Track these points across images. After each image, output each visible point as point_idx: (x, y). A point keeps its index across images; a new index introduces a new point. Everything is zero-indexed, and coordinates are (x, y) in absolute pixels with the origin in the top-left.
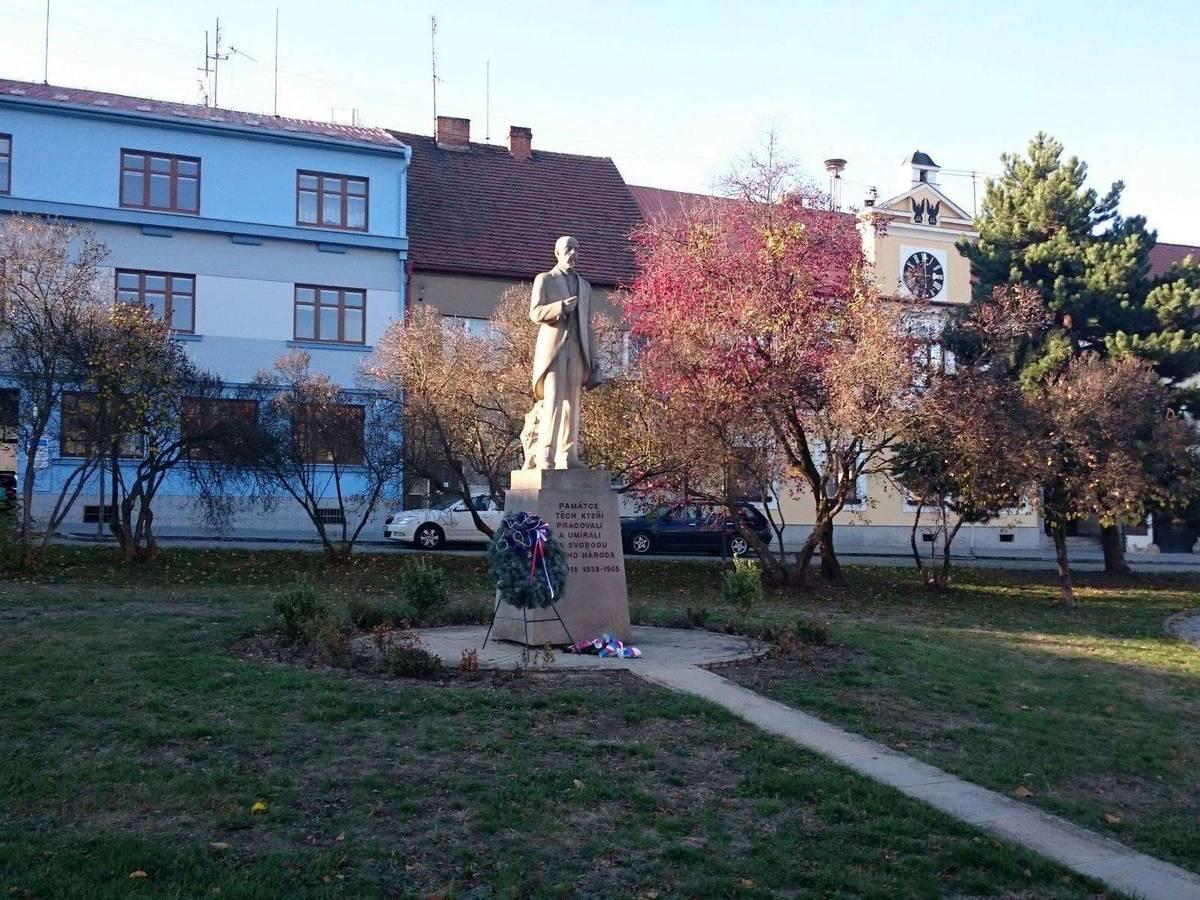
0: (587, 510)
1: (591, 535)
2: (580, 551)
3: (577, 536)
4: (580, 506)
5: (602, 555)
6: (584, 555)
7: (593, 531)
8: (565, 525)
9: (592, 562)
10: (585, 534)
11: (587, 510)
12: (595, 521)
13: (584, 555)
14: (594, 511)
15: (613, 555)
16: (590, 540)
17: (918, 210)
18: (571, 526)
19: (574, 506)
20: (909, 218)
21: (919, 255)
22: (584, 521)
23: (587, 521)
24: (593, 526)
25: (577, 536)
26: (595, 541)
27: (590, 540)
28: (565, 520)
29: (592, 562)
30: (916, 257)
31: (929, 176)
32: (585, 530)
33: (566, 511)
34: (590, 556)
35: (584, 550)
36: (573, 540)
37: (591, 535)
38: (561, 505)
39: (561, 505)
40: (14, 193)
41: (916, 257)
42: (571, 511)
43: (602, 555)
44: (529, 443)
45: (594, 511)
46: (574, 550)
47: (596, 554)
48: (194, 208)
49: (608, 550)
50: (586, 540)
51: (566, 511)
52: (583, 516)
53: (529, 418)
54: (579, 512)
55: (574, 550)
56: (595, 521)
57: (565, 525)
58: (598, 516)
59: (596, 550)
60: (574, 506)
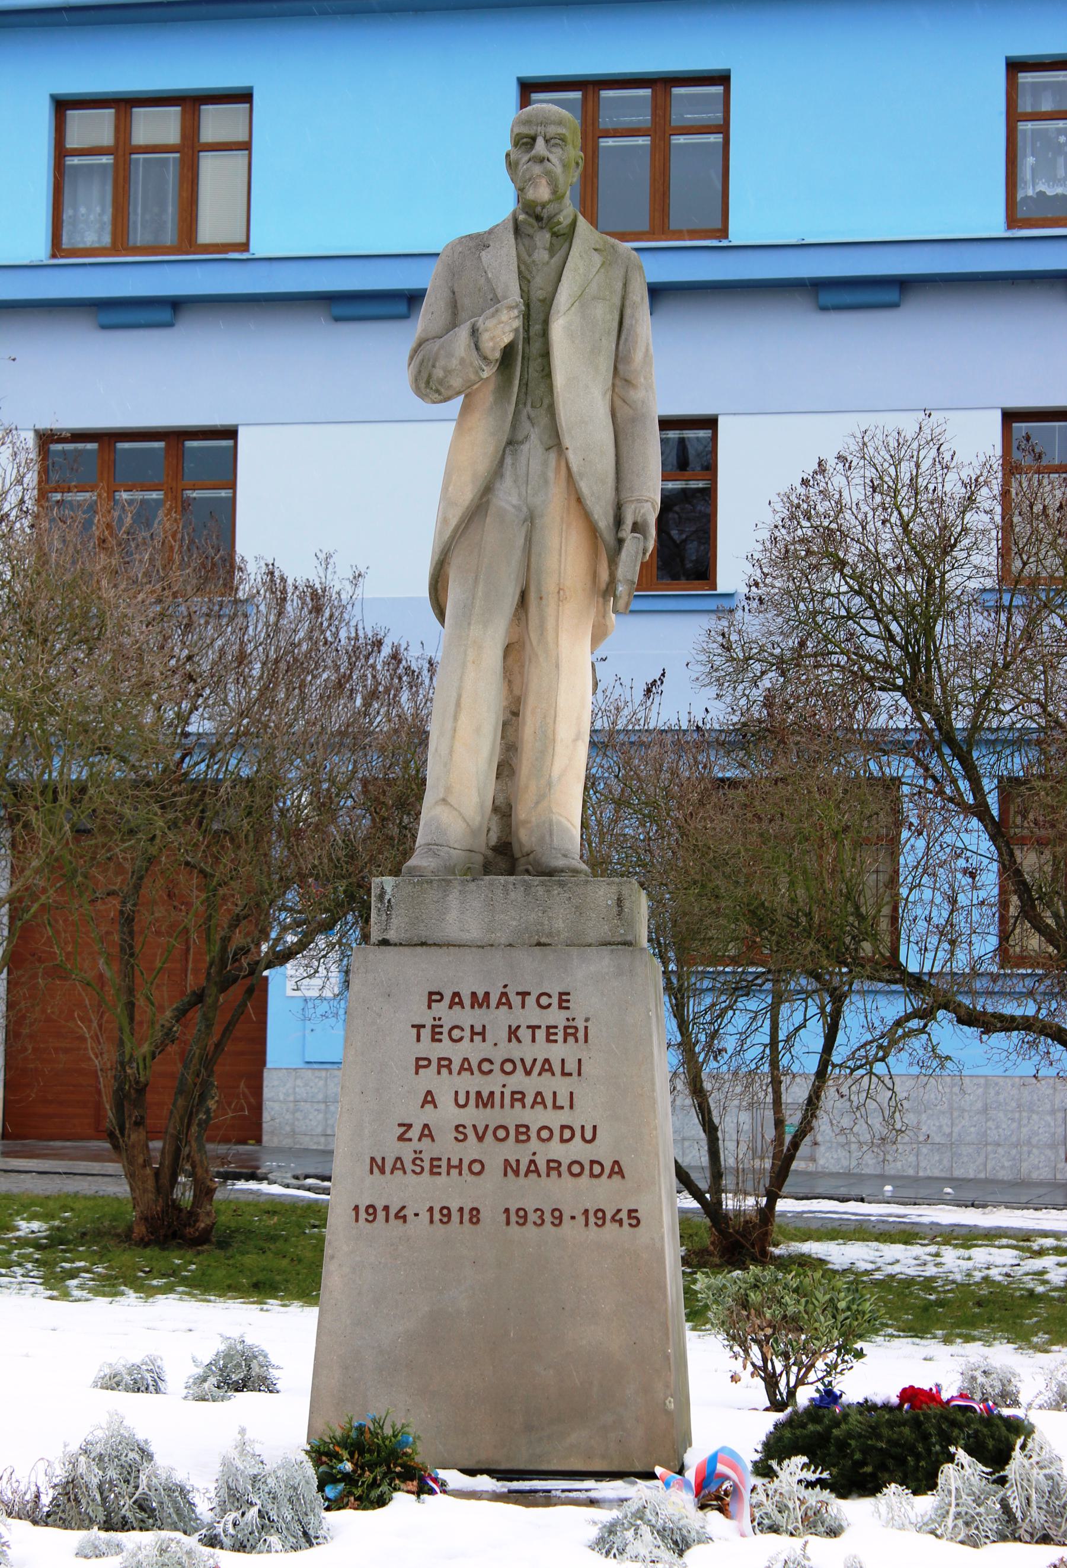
0: (532, 1015)
1: (539, 1099)
2: (495, 1154)
3: (485, 1101)
4: (504, 1000)
5: (576, 1169)
6: (511, 1168)
7: (547, 1084)
8: (444, 1064)
10: (517, 1097)
11: (532, 1015)
12: (557, 1052)
13: (511, 1168)
14: (556, 1017)
15: (617, 1170)
16: (536, 1117)
18: (466, 1066)
19: (480, 1001)
22: (516, 1051)
24: (547, 1066)
25: (485, 1101)
26: (555, 1119)
27: (536, 1117)
28: (445, 1048)
29: (532, 1193)
32: (518, 1081)
33: (449, 1016)
34: (532, 1168)
35: (511, 1150)
36: (472, 1116)
37: (539, 1099)
38: (434, 997)
39: (434, 997)
40: (258, 249)
42: (467, 1017)
43: (576, 1169)
45: (556, 1017)
46: (471, 1149)
47: (554, 1166)
48: (719, 225)
49: (603, 1150)
50: (514, 1116)
51: (449, 1016)
52: (513, 1033)
54: (498, 1020)
55: (471, 1149)
56: (557, 1052)
57: (444, 1064)
58: (570, 1032)
59: (556, 1150)
60: (480, 1001)
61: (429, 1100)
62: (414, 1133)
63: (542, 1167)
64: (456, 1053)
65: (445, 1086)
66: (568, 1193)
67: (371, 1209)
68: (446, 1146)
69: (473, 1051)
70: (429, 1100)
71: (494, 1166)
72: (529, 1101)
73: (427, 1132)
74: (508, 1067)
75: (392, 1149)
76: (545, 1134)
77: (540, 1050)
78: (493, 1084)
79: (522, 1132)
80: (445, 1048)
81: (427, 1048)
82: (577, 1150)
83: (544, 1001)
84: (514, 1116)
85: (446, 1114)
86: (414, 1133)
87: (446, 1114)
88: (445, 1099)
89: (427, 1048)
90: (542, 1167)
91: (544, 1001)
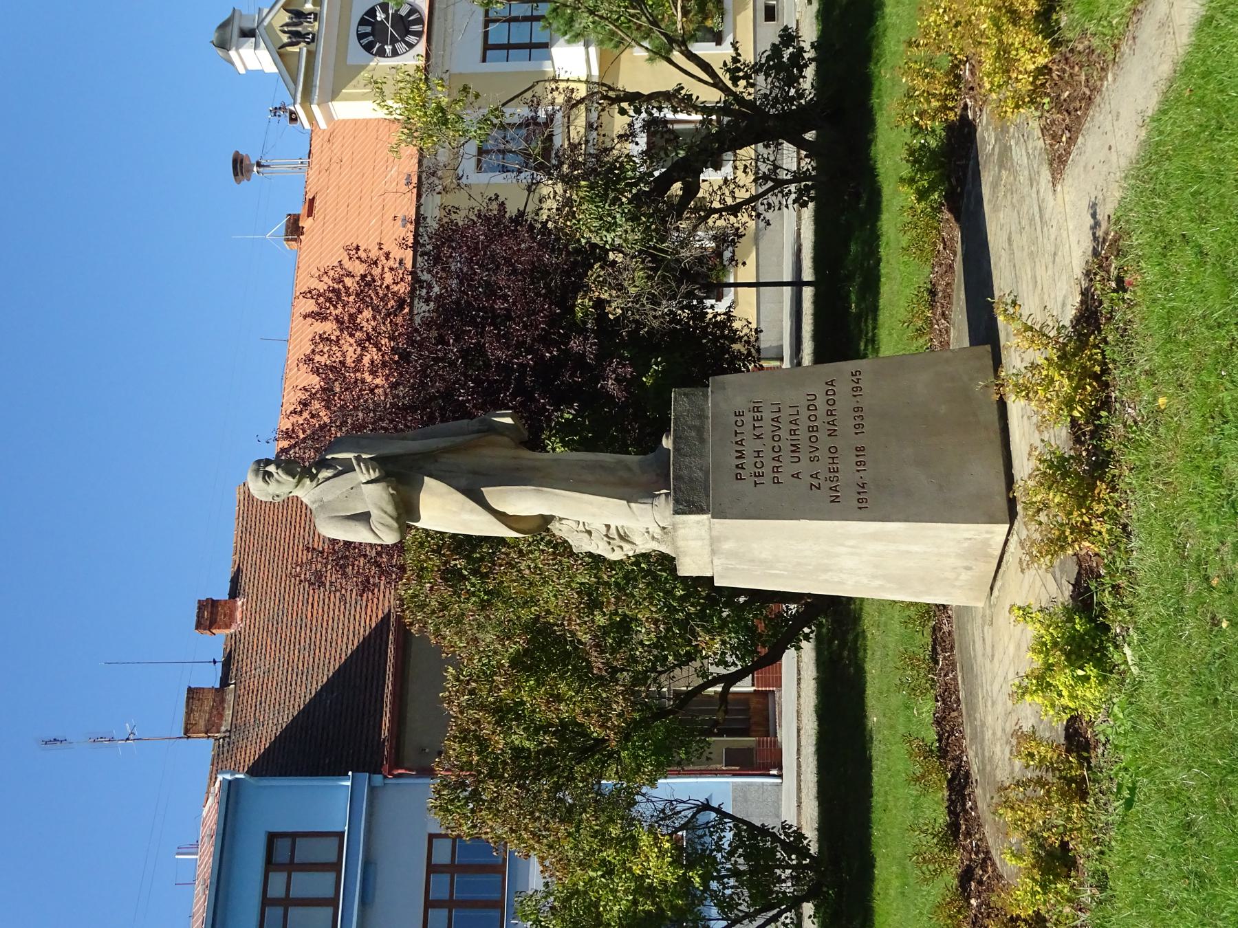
2: (824, 440)
3: (795, 449)
7: (785, 416)
8: (776, 470)
9: (846, 424)
10: (793, 432)
14: (748, 418)
16: (804, 423)
17: (297, 37)
20: (309, 52)
21: (360, 36)
23: (766, 427)
25: (795, 449)
26: (804, 413)
27: (804, 423)
28: (767, 470)
30: (365, 41)
31: (247, 25)
32: (784, 434)
33: (750, 469)
35: (822, 435)
36: (804, 455)
38: (738, 478)
41: (365, 41)
42: (748, 461)
44: (626, 546)
45: (748, 418)
46: (823, 454)
47: (830, 413)
49: (820, 390)
50: (803, 433)
51: (750, 469)
53: (582, 544)
54: (750, 447)
55: (823, 454)
56: (767, 415)
57: (776, 470)
61: (796, 476)
62: (815, 482)
63: (832, 418)
64: (770, 465)
65: (788, 468)
66: (844, 403)
67: (860, 501)
68: (822, 468)
69: (768, 455)
70: (796, 476)
71: (831, 442)
72: (794, 427)
73: (815, 476)
74: (776, 438)
75: (825, 493)
76: (813, 418)
77: (766, 427)
78: (786, 446)
79: (811, 429)
80: (767, 470)
81: (767, 480)
82: (820, 403)
83: (739, 423)
84: (803, 433)
85: (804, 466)
86: (815, 482)
87: (804, 466)
88: (796, 468)
89: (767, 480)
90: (832, 418)
91: (739, 423)
